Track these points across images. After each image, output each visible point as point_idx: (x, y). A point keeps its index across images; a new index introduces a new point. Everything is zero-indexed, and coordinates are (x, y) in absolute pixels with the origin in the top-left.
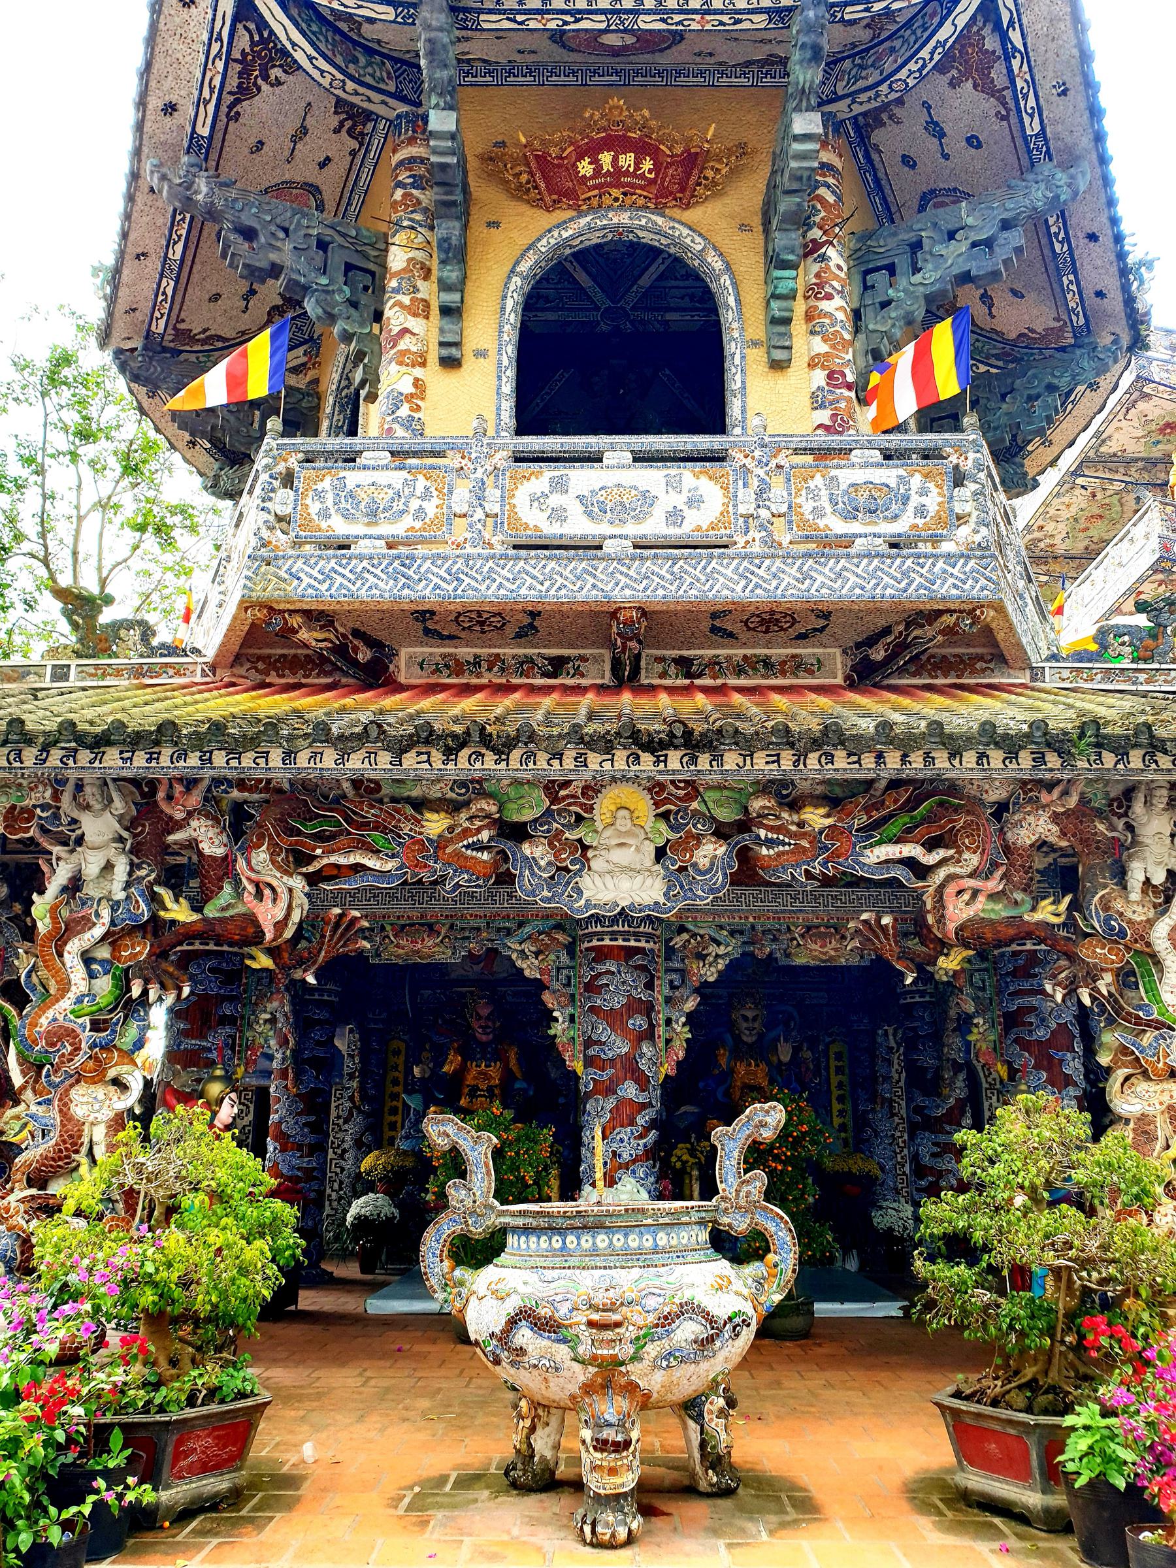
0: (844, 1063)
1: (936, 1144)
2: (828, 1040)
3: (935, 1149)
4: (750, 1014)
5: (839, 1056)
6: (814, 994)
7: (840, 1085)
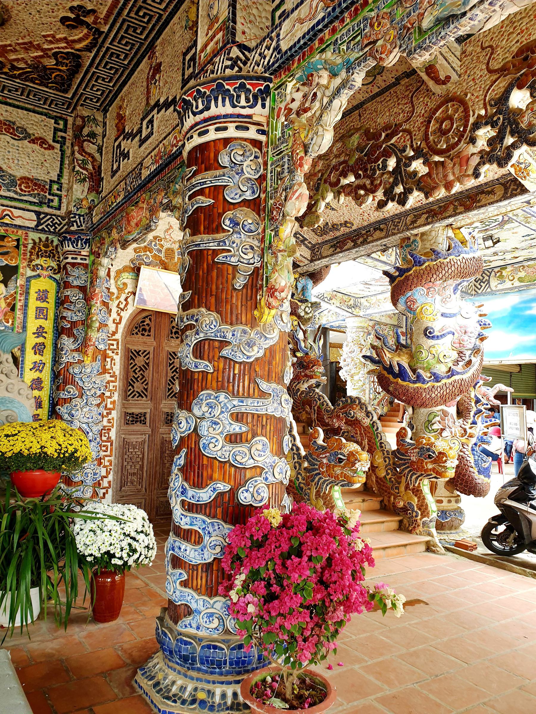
0: (51, 305)
1: (238, 417)
2: (30, 273)
3: (237, 428)
5: (43, 296)
7: (40, 332)
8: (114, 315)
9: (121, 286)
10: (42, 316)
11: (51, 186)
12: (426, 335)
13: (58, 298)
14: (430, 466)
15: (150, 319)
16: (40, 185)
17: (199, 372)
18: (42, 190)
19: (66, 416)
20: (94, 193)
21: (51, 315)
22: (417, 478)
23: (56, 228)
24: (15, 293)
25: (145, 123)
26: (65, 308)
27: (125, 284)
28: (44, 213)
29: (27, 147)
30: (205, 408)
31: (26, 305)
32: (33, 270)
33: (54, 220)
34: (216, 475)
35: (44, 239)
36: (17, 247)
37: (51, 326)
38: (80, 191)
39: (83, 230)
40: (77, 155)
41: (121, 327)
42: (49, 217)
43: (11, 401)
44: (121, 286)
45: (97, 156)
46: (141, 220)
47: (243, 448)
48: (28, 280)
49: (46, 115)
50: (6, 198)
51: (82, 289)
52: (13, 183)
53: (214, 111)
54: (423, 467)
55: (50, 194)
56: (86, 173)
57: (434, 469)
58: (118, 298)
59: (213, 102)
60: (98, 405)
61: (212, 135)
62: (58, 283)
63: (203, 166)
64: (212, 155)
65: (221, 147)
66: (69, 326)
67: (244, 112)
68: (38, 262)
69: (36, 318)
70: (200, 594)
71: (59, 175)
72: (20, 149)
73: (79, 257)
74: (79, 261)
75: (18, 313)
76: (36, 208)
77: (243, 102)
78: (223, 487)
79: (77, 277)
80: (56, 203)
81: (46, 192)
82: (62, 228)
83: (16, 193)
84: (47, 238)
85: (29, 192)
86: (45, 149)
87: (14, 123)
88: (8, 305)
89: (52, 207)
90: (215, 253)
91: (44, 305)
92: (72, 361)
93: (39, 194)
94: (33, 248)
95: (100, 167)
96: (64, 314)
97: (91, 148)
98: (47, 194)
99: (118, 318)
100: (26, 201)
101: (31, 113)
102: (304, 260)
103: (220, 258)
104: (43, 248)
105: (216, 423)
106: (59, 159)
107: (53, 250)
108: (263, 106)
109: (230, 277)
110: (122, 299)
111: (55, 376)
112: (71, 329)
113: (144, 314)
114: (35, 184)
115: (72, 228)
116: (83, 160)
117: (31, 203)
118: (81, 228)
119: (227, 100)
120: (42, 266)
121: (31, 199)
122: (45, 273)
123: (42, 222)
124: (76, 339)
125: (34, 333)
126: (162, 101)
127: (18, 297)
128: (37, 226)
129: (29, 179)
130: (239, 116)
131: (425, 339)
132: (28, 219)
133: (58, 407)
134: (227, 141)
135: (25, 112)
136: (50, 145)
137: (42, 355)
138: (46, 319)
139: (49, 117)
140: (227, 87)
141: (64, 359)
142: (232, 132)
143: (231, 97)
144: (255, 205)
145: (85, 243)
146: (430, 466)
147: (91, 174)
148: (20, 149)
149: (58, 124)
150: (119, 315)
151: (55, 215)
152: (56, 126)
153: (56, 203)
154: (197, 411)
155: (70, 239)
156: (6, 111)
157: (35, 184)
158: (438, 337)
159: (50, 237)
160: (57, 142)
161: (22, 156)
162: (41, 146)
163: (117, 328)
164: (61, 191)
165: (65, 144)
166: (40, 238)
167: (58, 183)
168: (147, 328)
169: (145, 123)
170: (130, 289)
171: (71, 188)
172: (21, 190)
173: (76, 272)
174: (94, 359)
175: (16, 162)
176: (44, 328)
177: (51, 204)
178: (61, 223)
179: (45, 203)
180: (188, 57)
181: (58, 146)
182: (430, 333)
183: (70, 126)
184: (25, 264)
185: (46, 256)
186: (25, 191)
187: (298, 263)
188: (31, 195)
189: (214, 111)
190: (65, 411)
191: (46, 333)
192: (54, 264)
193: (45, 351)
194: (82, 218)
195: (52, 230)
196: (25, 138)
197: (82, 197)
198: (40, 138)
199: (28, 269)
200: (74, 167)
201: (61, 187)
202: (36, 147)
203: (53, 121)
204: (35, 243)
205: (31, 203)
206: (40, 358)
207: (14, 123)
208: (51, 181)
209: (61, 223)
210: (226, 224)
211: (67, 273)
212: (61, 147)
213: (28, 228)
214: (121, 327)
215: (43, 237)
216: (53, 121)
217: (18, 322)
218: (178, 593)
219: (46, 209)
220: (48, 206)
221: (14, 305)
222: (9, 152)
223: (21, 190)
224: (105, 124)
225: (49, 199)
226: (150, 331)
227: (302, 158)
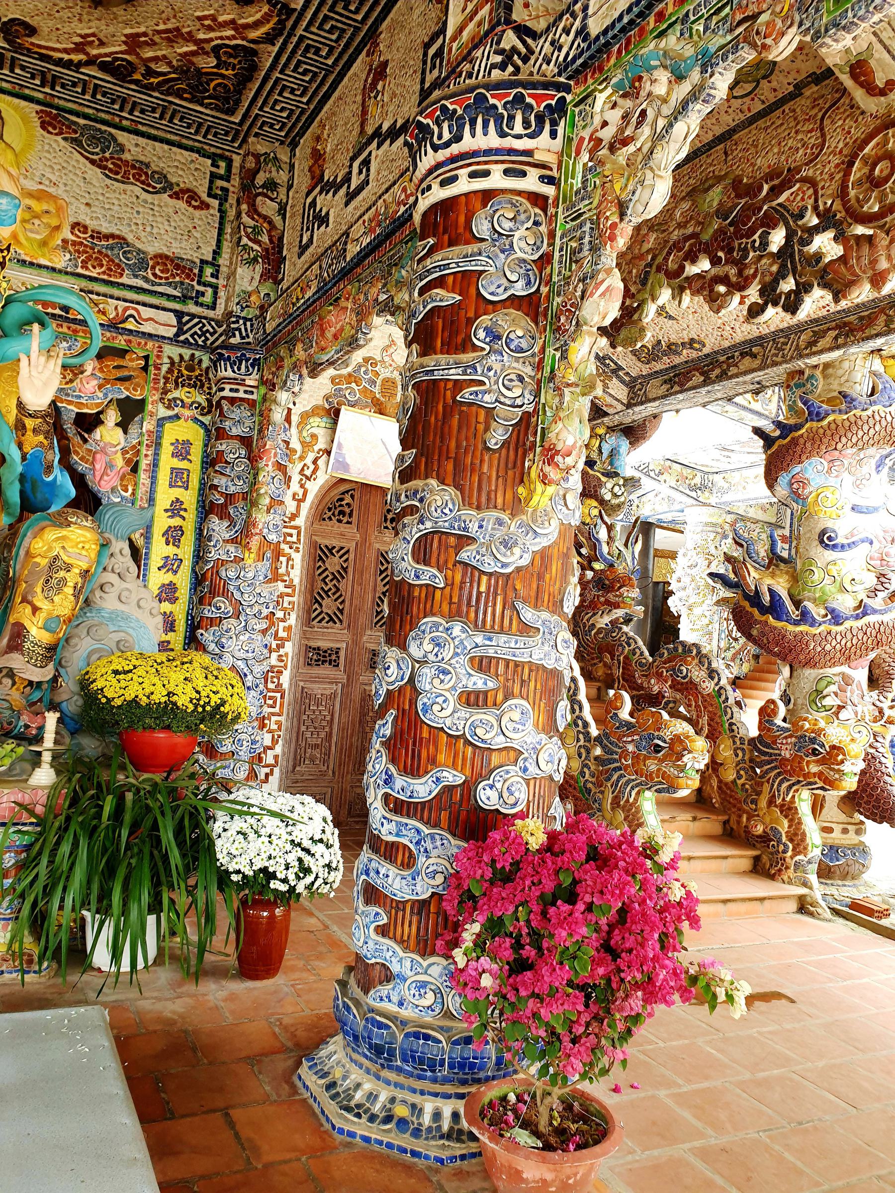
1: (482, 664)
2: (163, 412)
3: (478, 682)
5: (182, 450)
6: (146, 312)
7: (176, 508)
8: (295, 486)
9: (308, 439)
10: (180, 484)
11: (201, 270)
12: (822, 542)
13: (206, 455)
14: (814, 769)
15: (352, 496)
16: (185, 267)
17: (421, 585)
18: (188, 276)
19: (212, 647)
21: (195, 482)
22: (790, 787)
23: (207, 339)
24: (139, 443)
25: (356, 165)
26: (216, 471)
27: (314, 436)
28: (188, 314)
29: (166, 206)
30: (428, 647)
31: (155, 464)
32: (169, 407)
33: (204, 325)
34: (441, 758)
35: (187, 358)
36: (145, 369)
37: (194, 500)
38: (247, 278)
39: (249, 343)
40: (245, 219)
41: (305, 507)
42: (196, 320)
43: (127, 618)
44: (308, 439)
45: (277, 220)
46: (342, 329)
47: (487, 716)
48: (161, 423)
49: (198, 151)
50: (131, 288)
51: (246, 441)
52: (142, 263)
53: (468, 143)
54: (802, 769)
55: (199, 283)
56: (259, 249)
57: (820, 775)
58: (302, 458)
60: (264, 632)
61: (464, 185)
62: (207, 431)
63: (446, 237)
65: (478, 205)
66: (222, 501)
67: (519, 145)
68: (176, 394)
69: (171, 486)
70: (406, 949)
71: (215, 252)
72: (156, 208)
73: (242, 389)
74: (241, 395)
75: (143, 477)
76: (177, 306)
77: (518, 128)
78: (453, 777)
79: (239, 422)
80: (208, 298)
81: (193, 280)
82: (217, 339)
83: (146, 280)
84: (193, 355)
85: (167, 278)
86: (195, 207)
87: (148, 165)
88: (128, 462)
89: (202, 305)
90: (458, 386)
91: (184, 465)
92: (224, 557)
93: (182, 283)
94: (170, 371)
95: (281, 239)
96: (216, 482)
97: (268, 207)
98: (195, 283)
99: (301, 492)
100: (162, 294)
101: (174, 149)
102: (615, 403)
103: (466, 395)
104: (185, 372)
106: (217, 225)
107: (201, 375)
108: (553, 135)
110: (309, 460)
111: (198, 580)
112: (224, 506)
113: (343, 488)
114: (177, 267)
115: (232, 341)
116: (254, 228)
117: (169, 297)
118: (247, 340)
119: (492, 123)
120: (182, 401)
121: (170, 291)
122: (187, 413)
123: (185, 328)
124: (232, 523)
125: (166, 511)
126: (385, 127)
127: (144, 451)
128: (177, 335)
130: (511, 151)
131: (820, 549)
132: (162, 323)
133: (200, 631)
134: (487, 195)
135: (166, 147)
136: (202, 202)
137: (178, 547)
138: (187, 488)
139: (204, 156)
140: (492, 101)
141: (213, 555)
142: (497, 180)
143: (499, 119)
144: (530, 305)
145: (253, 366)
146: (814, 769)
147: (267, 250)
148: (156, 208)
149: (218, 167)
150: (302, 486)
151: (205, 318)
152: (214, 169)
153: (208, 298)
154: (414, 650)
155: (229, 358)
156: (137, 145)
157: (177, 267)
158: (843, 546)
159: (197, 354)
160: (215, 197)
161: (159, 219)
163: (298, 507)
164: (217, 278)
165: (226, 200)
166: (181, 356)
167: (213, 265)
168: (347, 510)
169: (356, 165)
170: (321, 444)
171: (234, 273)
172: (155, 275)
173: (237, 413)
174: (261, 557)
175: (148, 229)
176: (182, 503)
177: (201, 300)
178: (215, 332)
179: (191, 298)
180: (432, 51)
181: (215, 203)
182: (829, 538)
183: (235, 170)
184: (156, 397)
185: (189, 386)
186: (161, 278)
187: (604, 408)
188: (169, 284)
189: (468, 143)
190: (211, 638)
191: (185, 510)
192: (201, 399)
193: (182, 539)
194: (248, 324)
195: (200, 343)
196: (164, 190)
197: (250, 289)
199: (160, 405)
200: (240, 239)
201: (218, 271)
202: (181, 205)
203: (209, 162)
204: (172, 363)
205: (169, 297)
206: (175, 550)
207: (148, 165)
208: (202, 261)
209: (215, 332)
211: (222, 414)
212: (221, 205)
213: (163, 337)
214: (305, 507)
215: (187, 353)
216: (209, 162)
217: (142, 491)
218: (371, 944)
219: (192, 308)
220: (197, 303)
221: (137, 462)
222: (138, 212)
223: (155, 275)
224: (292, 167)
225: (198, 291)
226: (351, 515)
227: (614, 226)
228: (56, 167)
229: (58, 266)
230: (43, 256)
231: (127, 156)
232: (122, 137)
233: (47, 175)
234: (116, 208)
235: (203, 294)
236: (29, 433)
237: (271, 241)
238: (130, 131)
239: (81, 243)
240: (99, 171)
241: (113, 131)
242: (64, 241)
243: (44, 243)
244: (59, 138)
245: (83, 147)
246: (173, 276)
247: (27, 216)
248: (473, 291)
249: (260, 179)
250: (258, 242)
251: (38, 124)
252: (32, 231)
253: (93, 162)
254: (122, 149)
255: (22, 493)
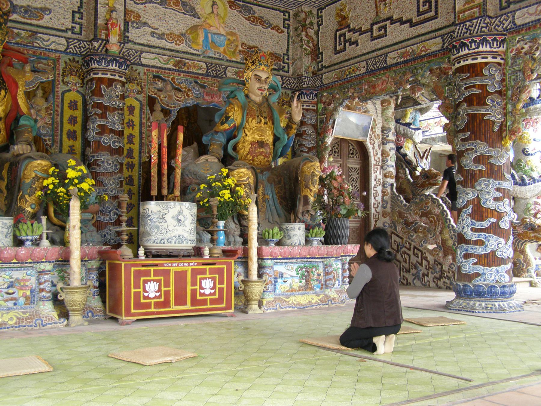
1: (498, 190)
4: (264, 76)
11: (283, 58)
12: (524, 153)
14: (532, 235)
15: (338, 145)
18: (279, 61)
20: (314, 62)
22: (522, 243)
26: (303, 138)
30: (483, 186)
34: (489, 216)
45: (314, 37)
47: (500, 203)
53: (481, 49)
54: (527, 236)
57: (535, 236)
59: (481, 46)
61: (480, 60)
63: (474, 74)
64: (479, 69)
65: (484, 66)
67: (495, 50)
70: (484, 266)
73: (311, 105)
77: (495, 46)
78: (493, 220)
80: (286, 69)
86: (279, 33)
90: (484, 115)
96: (303, 143)
98: (282, 63)
102: (426, 100)
103: (486, 118)
105: (489, 192)
108: (503, 47)
109: (491, 126)
114: (276, 57)
116: (307, 41)
119: (488, 45)
129: (272, 54)
130: (493, 52)
131: (523, 155)
134: (486, 64)
135: (268, 10)
136: (282, 30)
139: (281, 12)
140: (488, 39)
142: (490, 59)
143: (490, 43)
144: (500, 93)
146: (532, 235)
153: (286, 69)
154: (478, 188)
155: (306, 94)
157: (276, 57)
158: (532, 154)
160: (285, 28)
161: (268, 38)
162: (277, 31)
168: (337, 150)
181: (286, 30)
182: (527, 152)
183: (291, 16)
187: (420, 102)
189: (481, 49)
198: (277, 26)
200: (303, 45)
202: (275, 32)
203: (282, 14)
208: (284, 54)
210: (489, 102)
216: (282, 14)
218: (471, 268)
220: (283, 71)
226: (338, 152)
227: (530, 75)
228: (235, 22)
229: (238, 61)
230: (234, 57)
231: (256, 15)
232: (255, 8)
233: (233, 25)
234: (254, 35)
235: (284, 67)
236: (293, 130)
237: (313, 46)
238: (257, 5)
239: (244, 51)
240: (248, 22)
241: (251, 6)
242: (240, 51)
243: (234, 52)
244: (235, 11)
245: (242, 13)
246: (274, 61)
247: (229, 43)
248: (485, 89)
249: (307, 22)
250: (309, 47)
251: (228, 6)
252: (230, 48)
253: (246, 19)
254: (254, 13)
255: (282, 151)
